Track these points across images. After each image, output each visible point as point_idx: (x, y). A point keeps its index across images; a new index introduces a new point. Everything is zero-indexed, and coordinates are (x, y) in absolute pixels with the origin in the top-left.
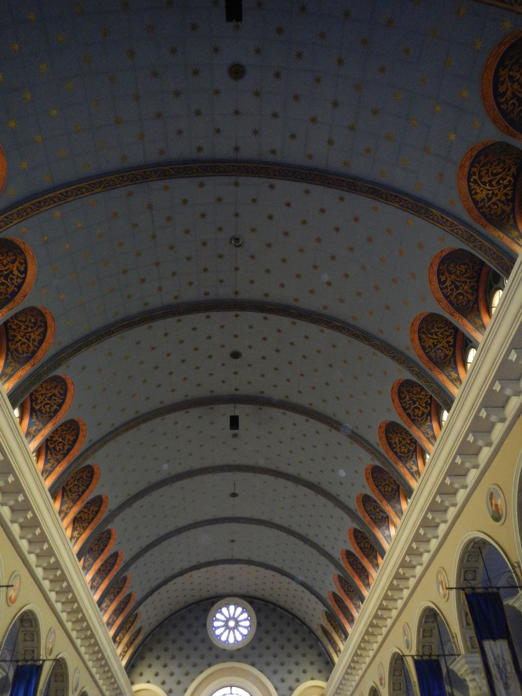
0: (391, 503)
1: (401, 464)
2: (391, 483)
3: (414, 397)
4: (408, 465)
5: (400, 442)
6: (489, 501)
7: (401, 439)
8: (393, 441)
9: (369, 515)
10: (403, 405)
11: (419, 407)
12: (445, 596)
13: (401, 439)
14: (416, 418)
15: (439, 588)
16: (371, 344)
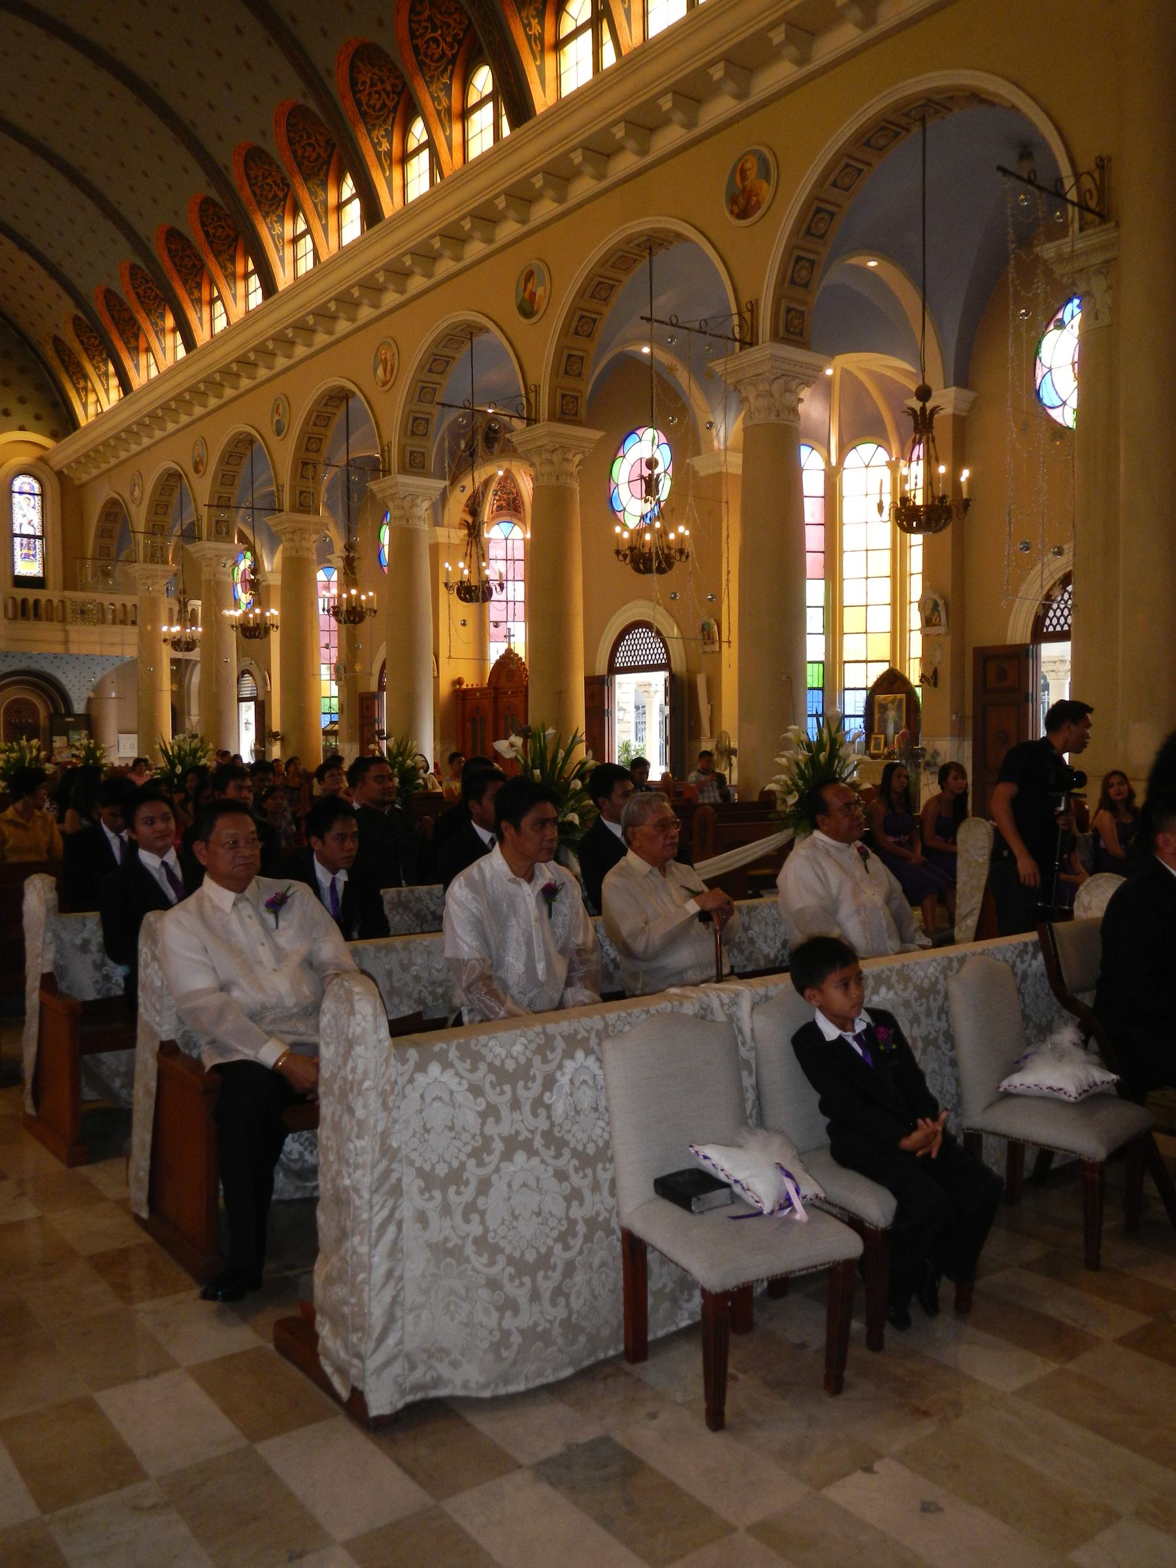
0: (310, 185)
1: (364, 130)
4: (375, 134)
5: (373, 85)
6: (522, 282)
9: (251, 185)
10: (413, 25)
12: (384, 384)
13: (376, 78)
14: (428, 61)
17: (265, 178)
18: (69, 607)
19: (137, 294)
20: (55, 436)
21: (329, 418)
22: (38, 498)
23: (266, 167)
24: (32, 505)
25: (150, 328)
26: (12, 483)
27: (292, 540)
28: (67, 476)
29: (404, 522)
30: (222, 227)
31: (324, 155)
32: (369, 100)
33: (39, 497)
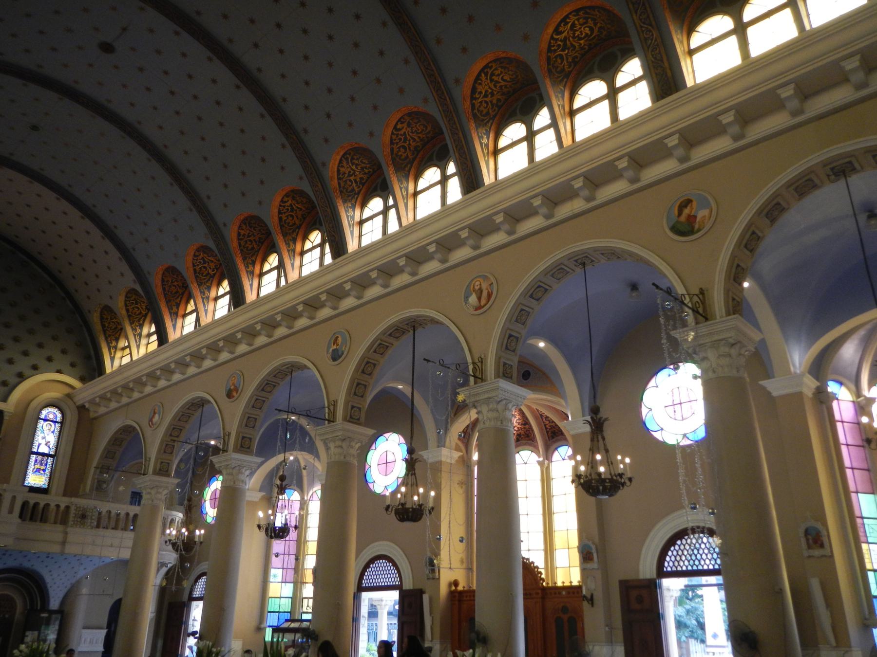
2: (409, 148)
3: (569, 40)
5: (486, 96)
7: (490, 91)
8: (480, 88)
9: (339, 179)
11: (565, 58)
13: (490, 91)
15: (466, 298)
17: (350, 176)
18: (73, 509)
19: (195, 270)
20: (82, 379)
21: (387, 347)
22: (58, 425)
23: (354, 167)
24: (52, 429)
25: (199, 294)
26: (40, 412)
27: (341, 447)
28: (88, 410)
29: (499, 423)
30: (292, 216)
31: (411, 157)
32: (480, 106)
33: (59, 425)
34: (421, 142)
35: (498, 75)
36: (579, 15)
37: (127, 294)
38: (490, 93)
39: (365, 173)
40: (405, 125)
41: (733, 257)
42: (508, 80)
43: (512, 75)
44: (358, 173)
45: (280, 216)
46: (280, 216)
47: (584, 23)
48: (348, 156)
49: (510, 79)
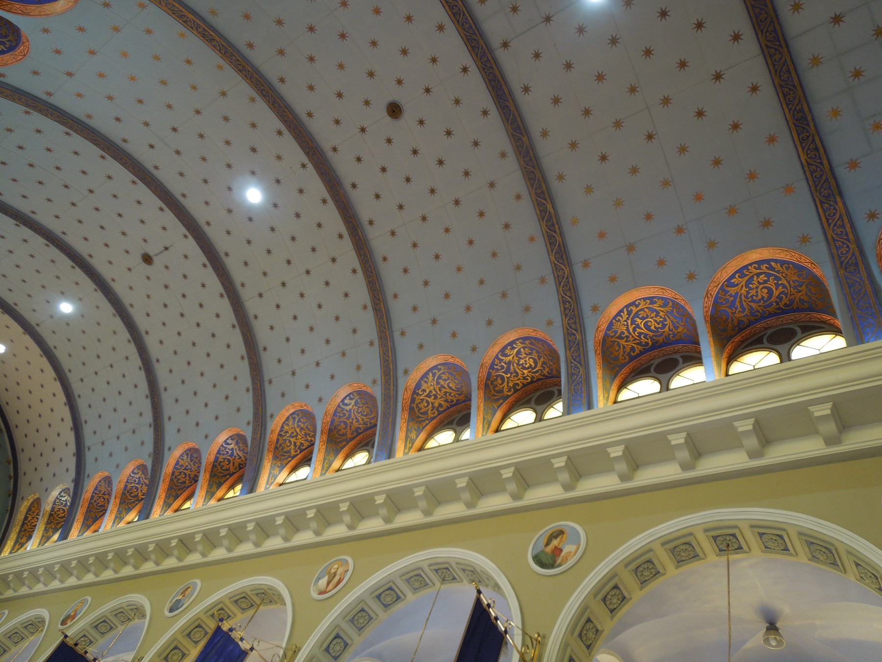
2: (351, 427)
3: (514, 366)
5: (429, 396)
7: (434, 392)
8: (424, 386)
9: (279, 435)
10: (496, 360)
12: (321, 593)
13: (434, 392)
14: (491, 388)
15: (319, 579)
16: (555, 264)
23: (298, 430)
31: (349, 436)
32: (420, 403)
34: (363, 426)
35: (445, 380)
36: (525, 344)
37: (61, 492)
38: (434, 395)
39: (307, 440)
40: (353, 402)
41: (584, 608)
42: (454, 388)
43: (458, 385)
44: (300, 437)
45: (218, 455)
46: (218, 455)
47: (531, 354)
48: (296, 416)
49: (456, 388)
